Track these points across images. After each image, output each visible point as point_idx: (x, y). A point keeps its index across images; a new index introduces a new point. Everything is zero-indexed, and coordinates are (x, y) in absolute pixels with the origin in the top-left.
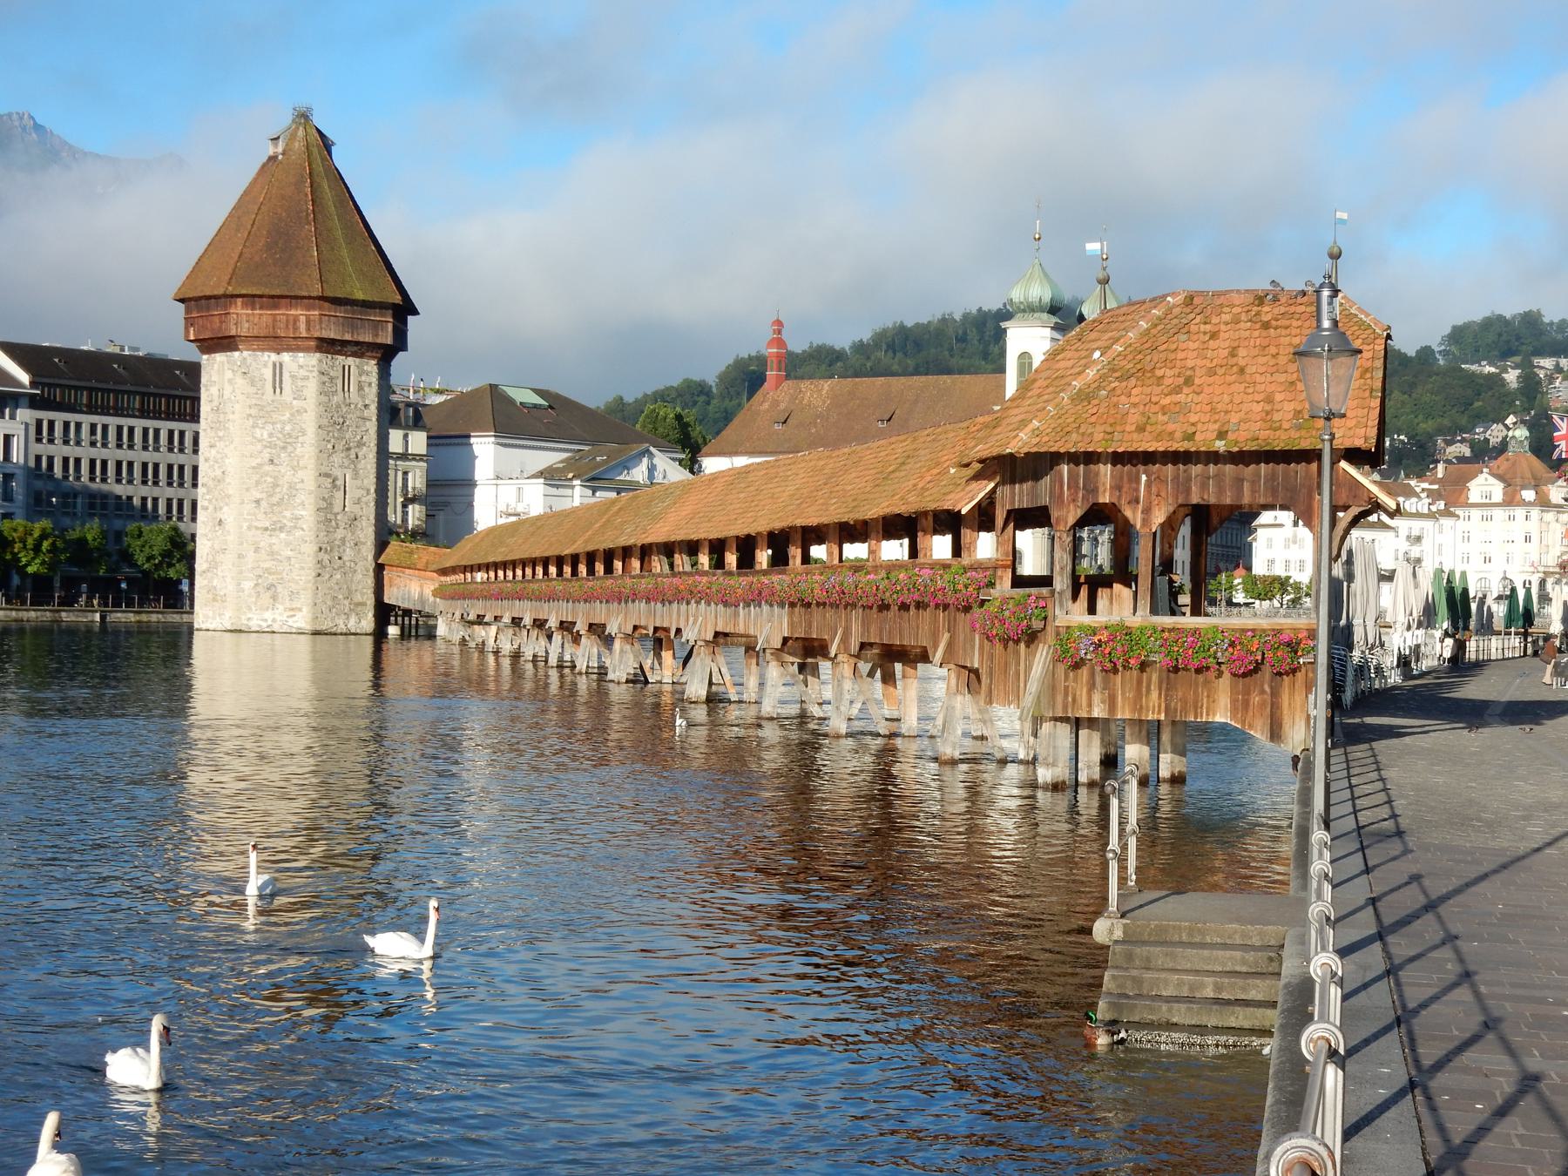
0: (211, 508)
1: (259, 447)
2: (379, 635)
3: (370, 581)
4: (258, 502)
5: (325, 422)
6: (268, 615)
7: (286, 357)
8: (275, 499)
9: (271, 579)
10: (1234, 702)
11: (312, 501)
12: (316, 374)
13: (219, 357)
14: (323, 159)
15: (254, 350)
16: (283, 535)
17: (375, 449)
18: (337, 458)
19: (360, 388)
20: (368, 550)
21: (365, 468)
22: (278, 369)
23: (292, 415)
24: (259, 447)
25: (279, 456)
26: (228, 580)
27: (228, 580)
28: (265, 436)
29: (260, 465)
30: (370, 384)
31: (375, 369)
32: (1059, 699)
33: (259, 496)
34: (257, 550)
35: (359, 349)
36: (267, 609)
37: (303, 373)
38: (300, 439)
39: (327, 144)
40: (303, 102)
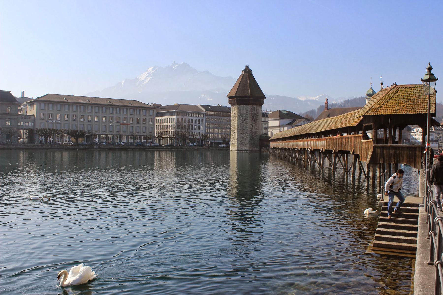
4: (240, 129)
5: (251, 116)
6: (242, 148)
8: (243, 129)
9: (242, 142)
18: (253, 122)
19: (257, 110)
22: (243, 108)
23: (246, 115)
29: (241, 123)
34: (240, 137)
36: (241, 147)
37: (247, 108)
40: (247, 64)
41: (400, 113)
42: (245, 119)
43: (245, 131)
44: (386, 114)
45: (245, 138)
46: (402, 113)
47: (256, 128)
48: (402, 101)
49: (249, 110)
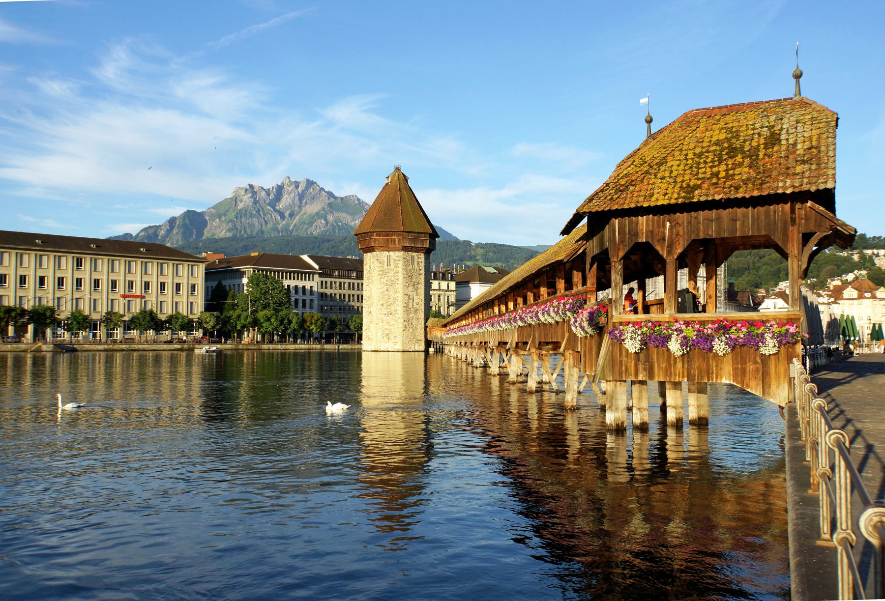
2: (426, 351)
3: (423, 332)
6: (387, 345)
7: (391, 253)
8: (389, 304)
9: (387, 332)
10: (735, 369)
13: (369, 254)
14: (404, 184)
18: (410, 289)
19: (418, 264)
20: (422, 321)
22: (389, 258)
31: (423, 257)
32: (617, 368)
34: (382, 322)
35: (417, 250)
37: (397, 259)
39: (406, 179)
40: (397, 164)
41: (703, 199)
42: (393, 282)
44: (653, 204)
45: (394, 322)
46: (710, 199)
47: (418, 301)
48: (709, 160)
49: (401, 263)
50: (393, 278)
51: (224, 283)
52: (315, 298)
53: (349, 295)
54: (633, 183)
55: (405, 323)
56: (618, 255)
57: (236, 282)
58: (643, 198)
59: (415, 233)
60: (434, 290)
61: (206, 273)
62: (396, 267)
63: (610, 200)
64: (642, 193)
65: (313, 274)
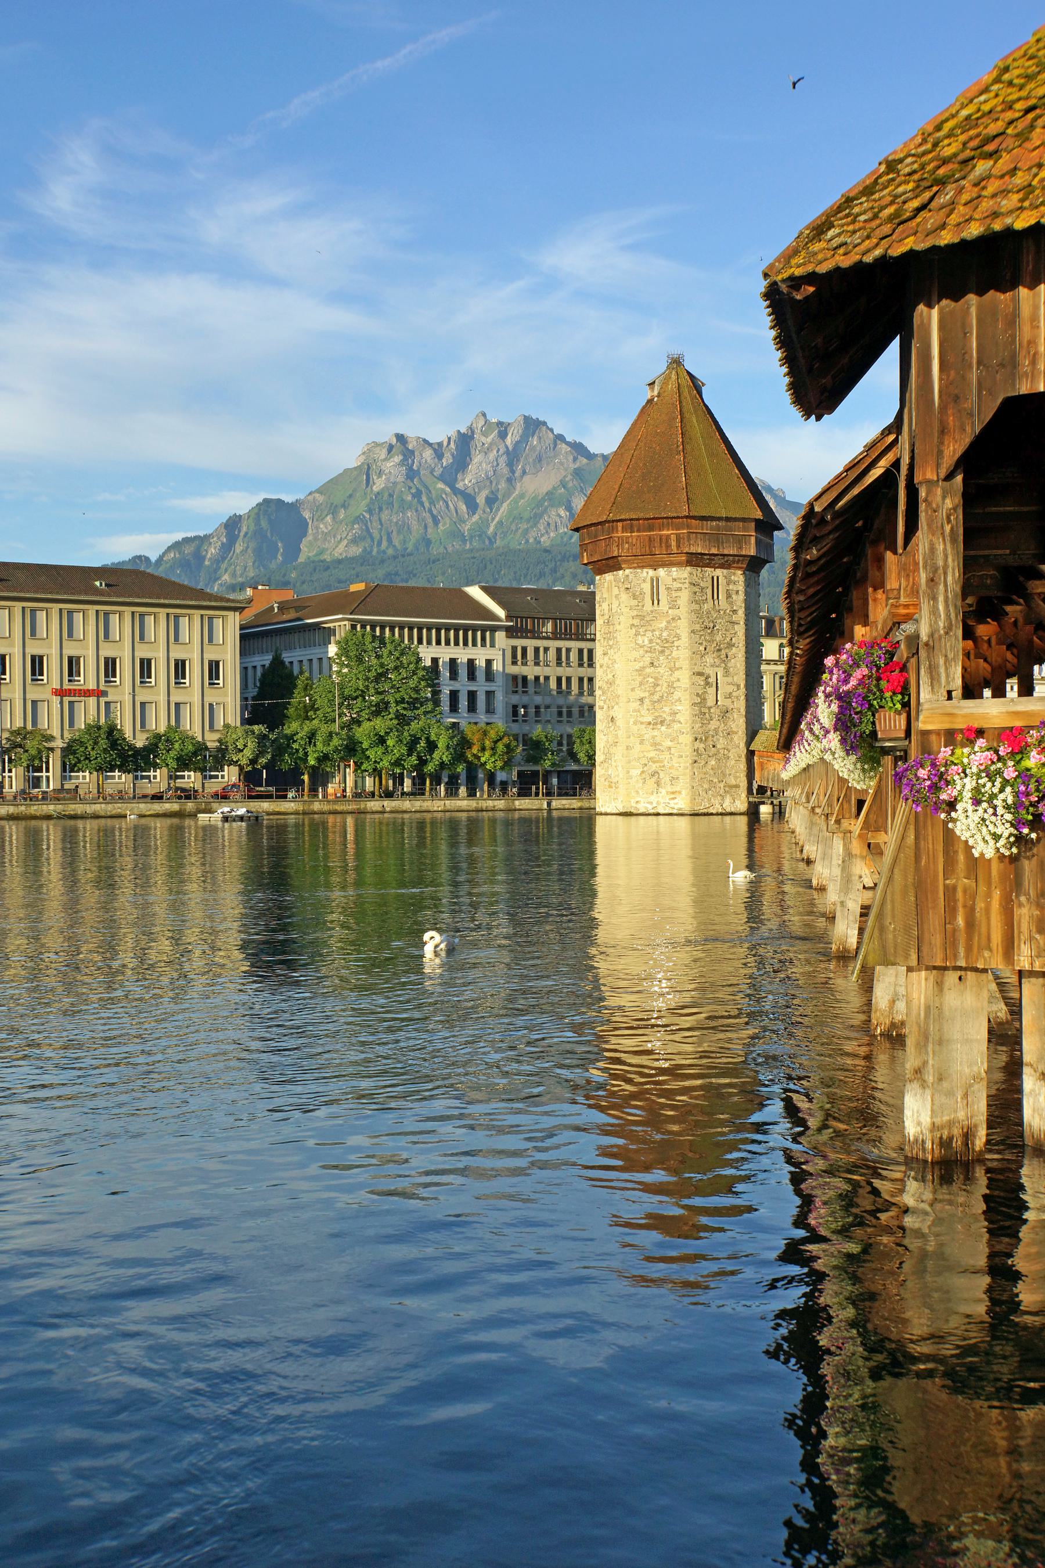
0: (606, 707)
1: (642, 652)
2: (753, 813)
3: (743, 766)
4: (641, 700)
5: (697, 627)
6: (653, 798)
7: (662, 572)
8: (656, 697)
9: (654, 767)
11: (688, 697)
12: (687, 585)
13: (608, 577)
14: (693, 398)
15: (635, 568)
16: (663, 728)
17: (743, 649)
18: (709, 659)
19: (729, 596)
20: (740, 739)
21: (735, 666)
22: (655, 583)
23: (668, 622)
24: (642, 652)
25: (658, 659)
26: (620, 769)
27: (620, 769)
28: (646, 642)
30: (737, 592)
31: (742, 579)
32: (934, 920)
33: (643, 695)
34: (642, 742)
35: (726, 562)
37: (676, 585)
38: (676, 644)
39: (696, 386)
40: (675, 350)
42: (666, 645)
43: (667, 709)
45: (670, 744)
47: (730, 689)
50: (665, 634)
51: (287, 657)
52: (499, 688)
53: (581, 680)
54: (990, 148)
55: (697, 744)
56: (940, 453)
57: (314, 653)
58: (1015, 197)
59: (719, 519)
60: (768, 662)
61: (243, 638)
62: (674, 606)
63: (890, 219)
64: (1020, 179)
65: (494, 629)
